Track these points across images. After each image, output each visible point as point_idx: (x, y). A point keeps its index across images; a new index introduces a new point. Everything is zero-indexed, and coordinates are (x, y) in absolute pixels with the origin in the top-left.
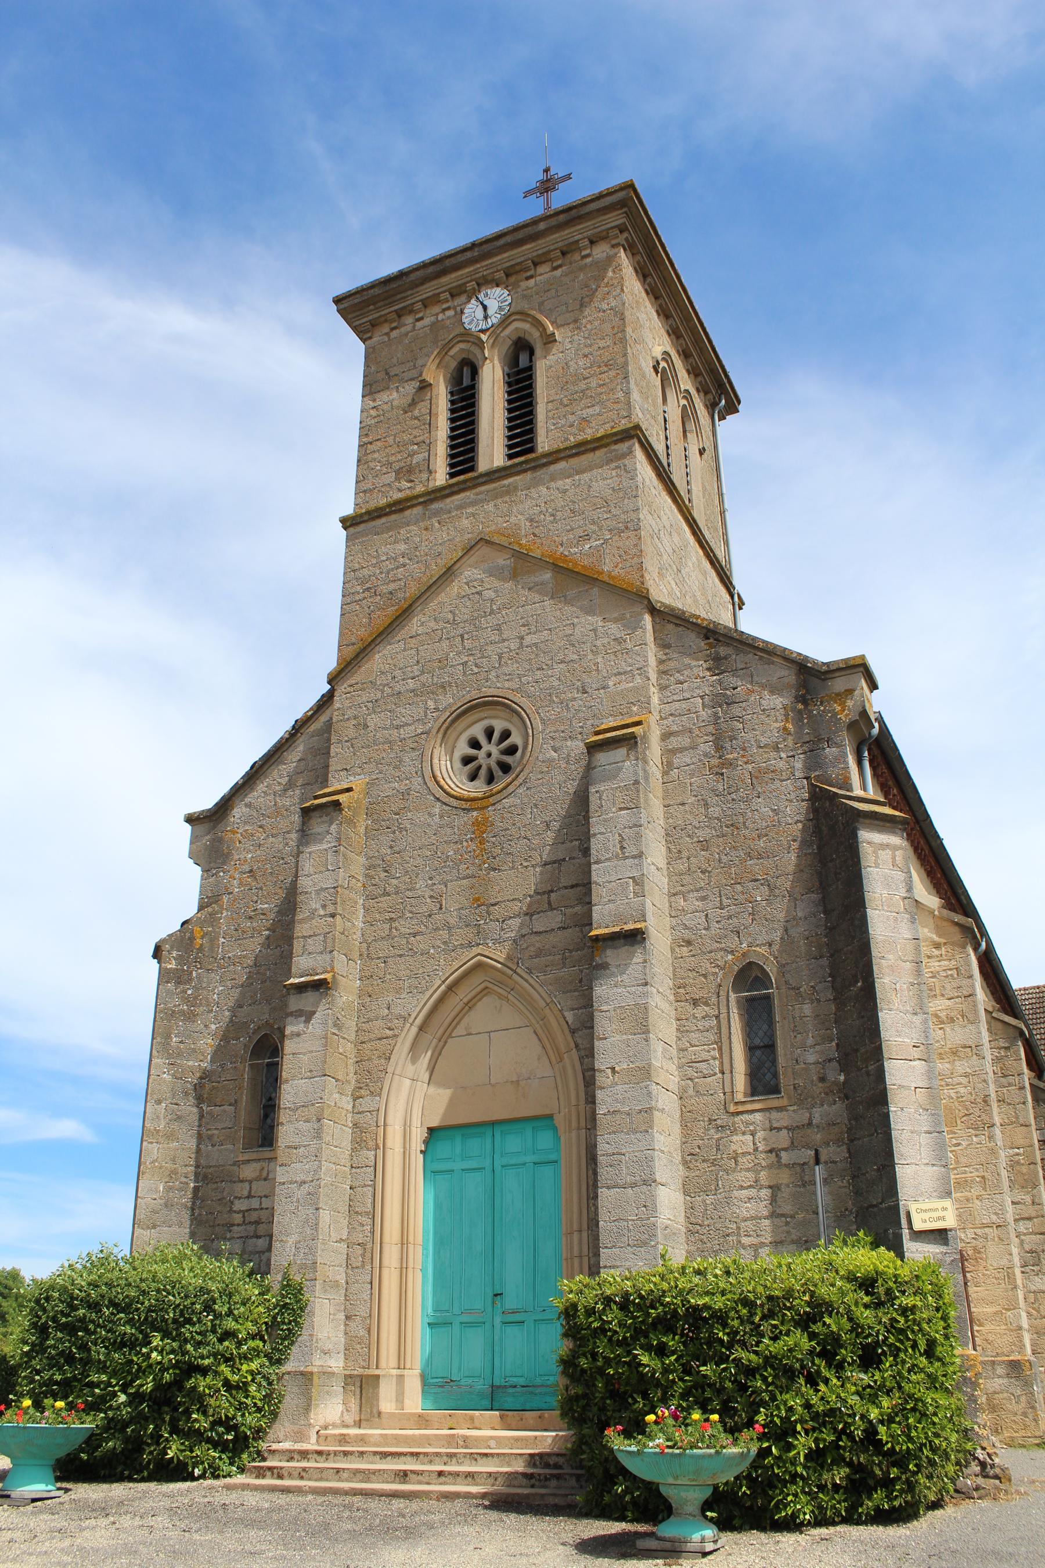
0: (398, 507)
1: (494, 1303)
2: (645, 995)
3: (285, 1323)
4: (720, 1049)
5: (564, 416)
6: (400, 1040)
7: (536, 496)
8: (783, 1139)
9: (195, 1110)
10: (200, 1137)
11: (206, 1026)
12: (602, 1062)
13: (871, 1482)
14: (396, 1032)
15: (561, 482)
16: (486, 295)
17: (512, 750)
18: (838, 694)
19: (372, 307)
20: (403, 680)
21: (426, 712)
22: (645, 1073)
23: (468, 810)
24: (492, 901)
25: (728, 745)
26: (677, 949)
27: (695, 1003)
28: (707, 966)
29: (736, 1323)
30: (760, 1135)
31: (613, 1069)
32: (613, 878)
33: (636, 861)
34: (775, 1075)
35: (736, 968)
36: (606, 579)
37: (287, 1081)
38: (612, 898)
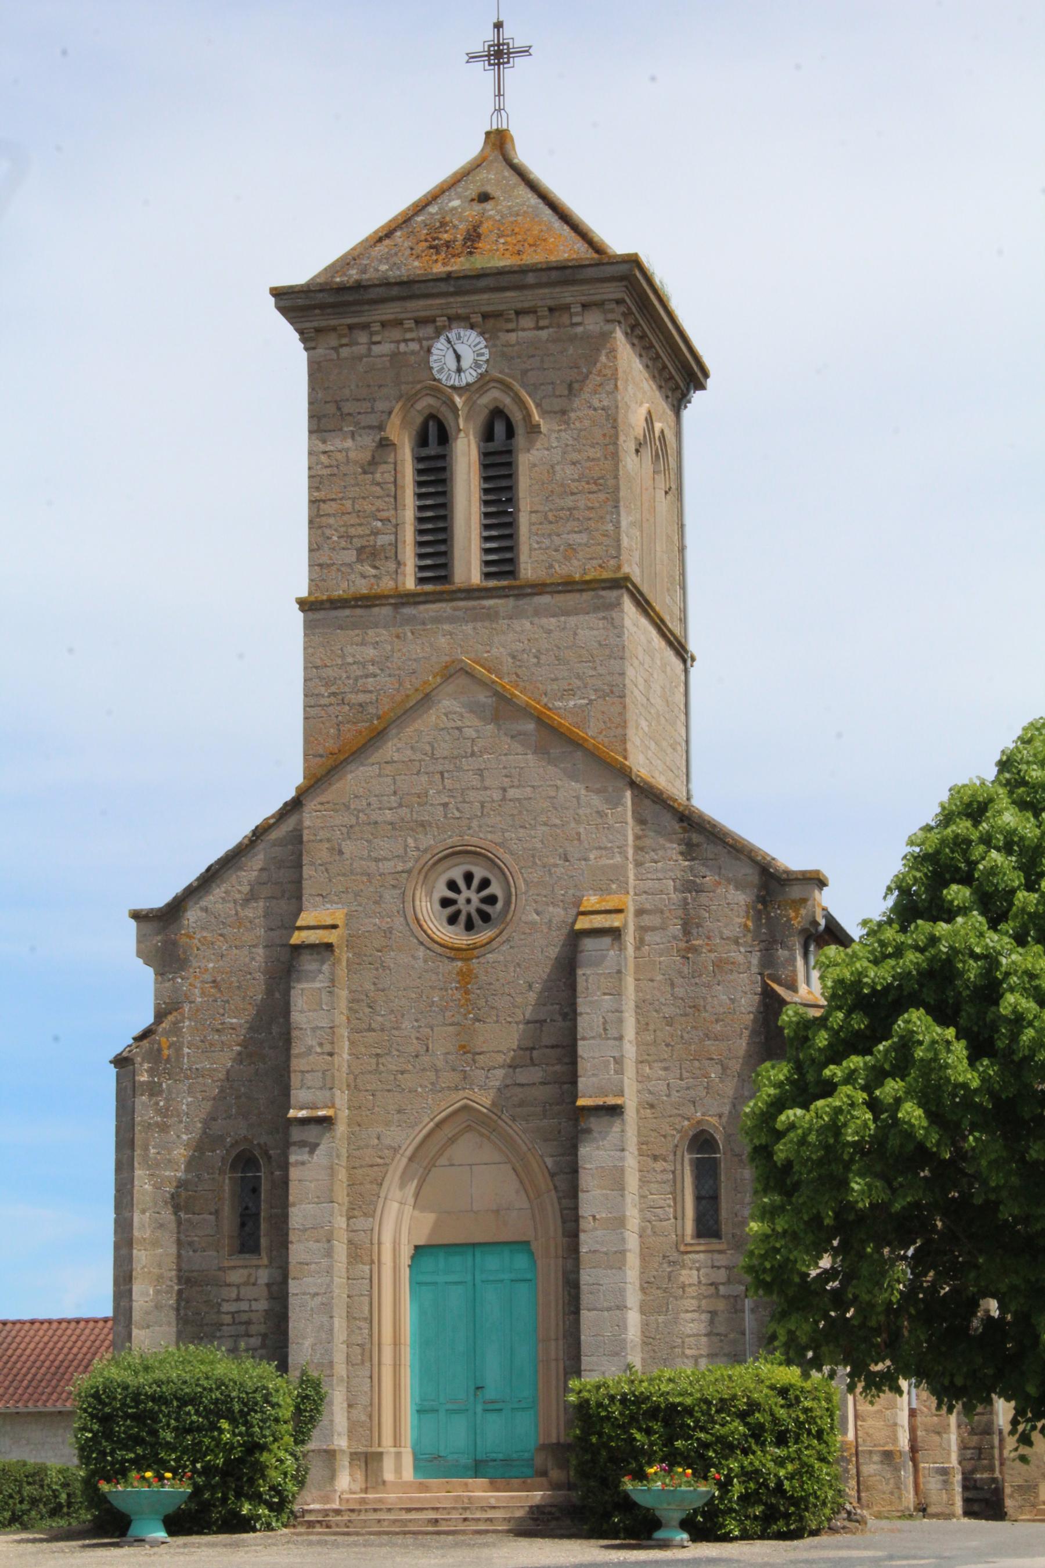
0: (365, 603)
1: (475, 1395)
2: (622, 1159)
3: (308, 1410)
4: (675, 1199)
5: (550, 535)
6: (391, 1168)
7: (519, 629)
8: (722, 1275)
9: (173, 1217)
10: (179, 1243)
11: (178, 1137)
12: (585, 1210)
13: (777, 1515)
14: (387, 1161)
15: (544, 621)
16: (459, 338)
17: (492, 900)
18: (794, 901)
19: (317, 311)
20: (380, 809)
21: (406, 850)
22: (620, 1222)
23: (452, 959)
24: (478, 1050)
25: (694, 931)
26: (642, 1111)
27: (655, 1158)
28: (667, 1129)
29: (699, 1414)
30: (702, 1271)
31: (594, 1217)
32: (597, 1055)
33: (617, 1043)
34: (717, 1222)
35: (691, 1133)
36: (590, 747)
37: (294, 1205)
38: (596, 1072)
